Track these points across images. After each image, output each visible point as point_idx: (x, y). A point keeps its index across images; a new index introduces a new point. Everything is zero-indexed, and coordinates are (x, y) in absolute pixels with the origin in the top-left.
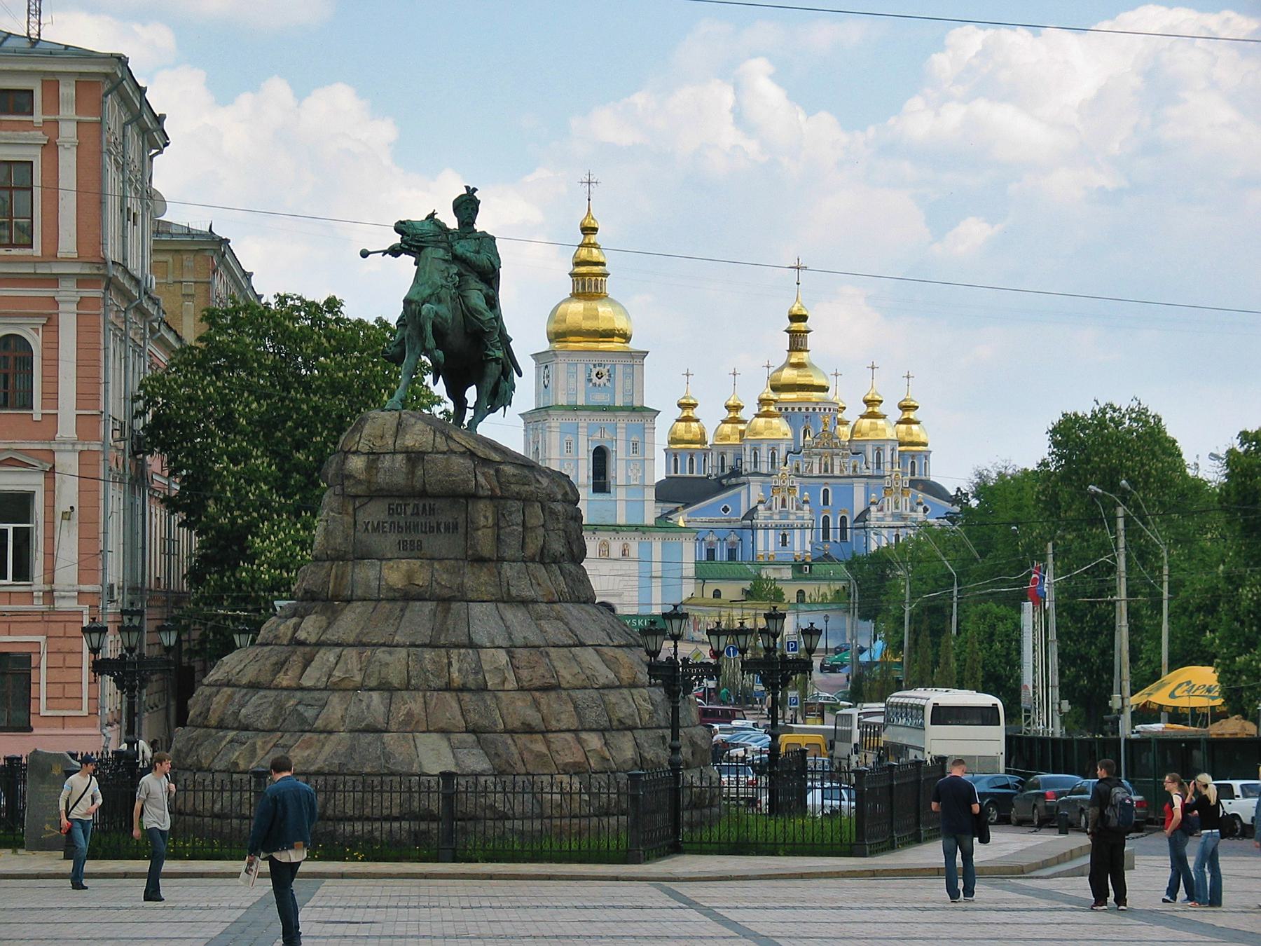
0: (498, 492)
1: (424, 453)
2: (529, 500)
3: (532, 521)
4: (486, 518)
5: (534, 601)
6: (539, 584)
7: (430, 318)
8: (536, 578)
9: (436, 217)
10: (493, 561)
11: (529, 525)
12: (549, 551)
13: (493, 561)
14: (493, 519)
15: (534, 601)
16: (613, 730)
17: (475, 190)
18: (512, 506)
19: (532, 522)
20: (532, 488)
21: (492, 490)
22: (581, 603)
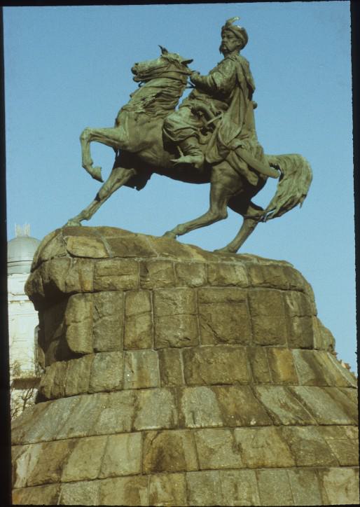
5: (116, 390)
7: (83, 139)
15: (116, 390)
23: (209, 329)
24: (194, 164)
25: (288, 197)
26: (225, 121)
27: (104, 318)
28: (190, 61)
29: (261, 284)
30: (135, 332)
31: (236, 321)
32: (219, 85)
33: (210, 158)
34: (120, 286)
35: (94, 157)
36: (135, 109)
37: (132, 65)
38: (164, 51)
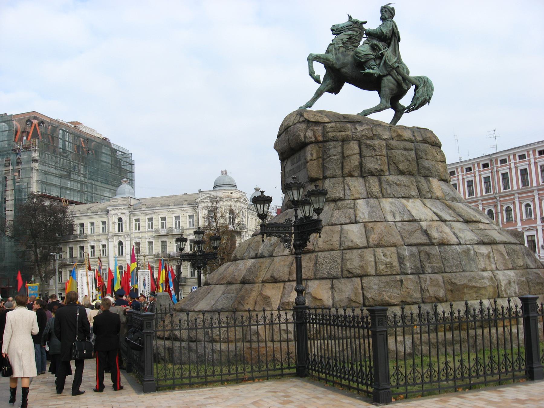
0: (320, 139)
1: (289, 127)
2: (347, 140)
3: (348, 152)
4: (312, 154)
5: (340, 199)
6: (350, 189)
7: (309, 59)
8: (348, 186)
9: (354, 18)
10: (320, 179)
11: (345, 155)
12: (365, 169)
13: (320, 179)
14: (317, 154)
15: (340, 199)
16: (343, 278)
17: (390, 4)
18: (330, 145)
19: (347, 152)
20: (349, 133)
21: (316, 138)
22: (398, 198)
23: (394, 165)
24: (374, 74)
25: (423, 98)
26: (388, 52)
27: (331, 157)
28: (365, 23)
29: (421, 141)
30: (351, 166)
31: (410, 161)
32: (385, 33)
33: (381, 72)
34: (340, 138)
35: (315, 69)
36: (338, 44)
37: (331, 26)
38: (350, 18)
